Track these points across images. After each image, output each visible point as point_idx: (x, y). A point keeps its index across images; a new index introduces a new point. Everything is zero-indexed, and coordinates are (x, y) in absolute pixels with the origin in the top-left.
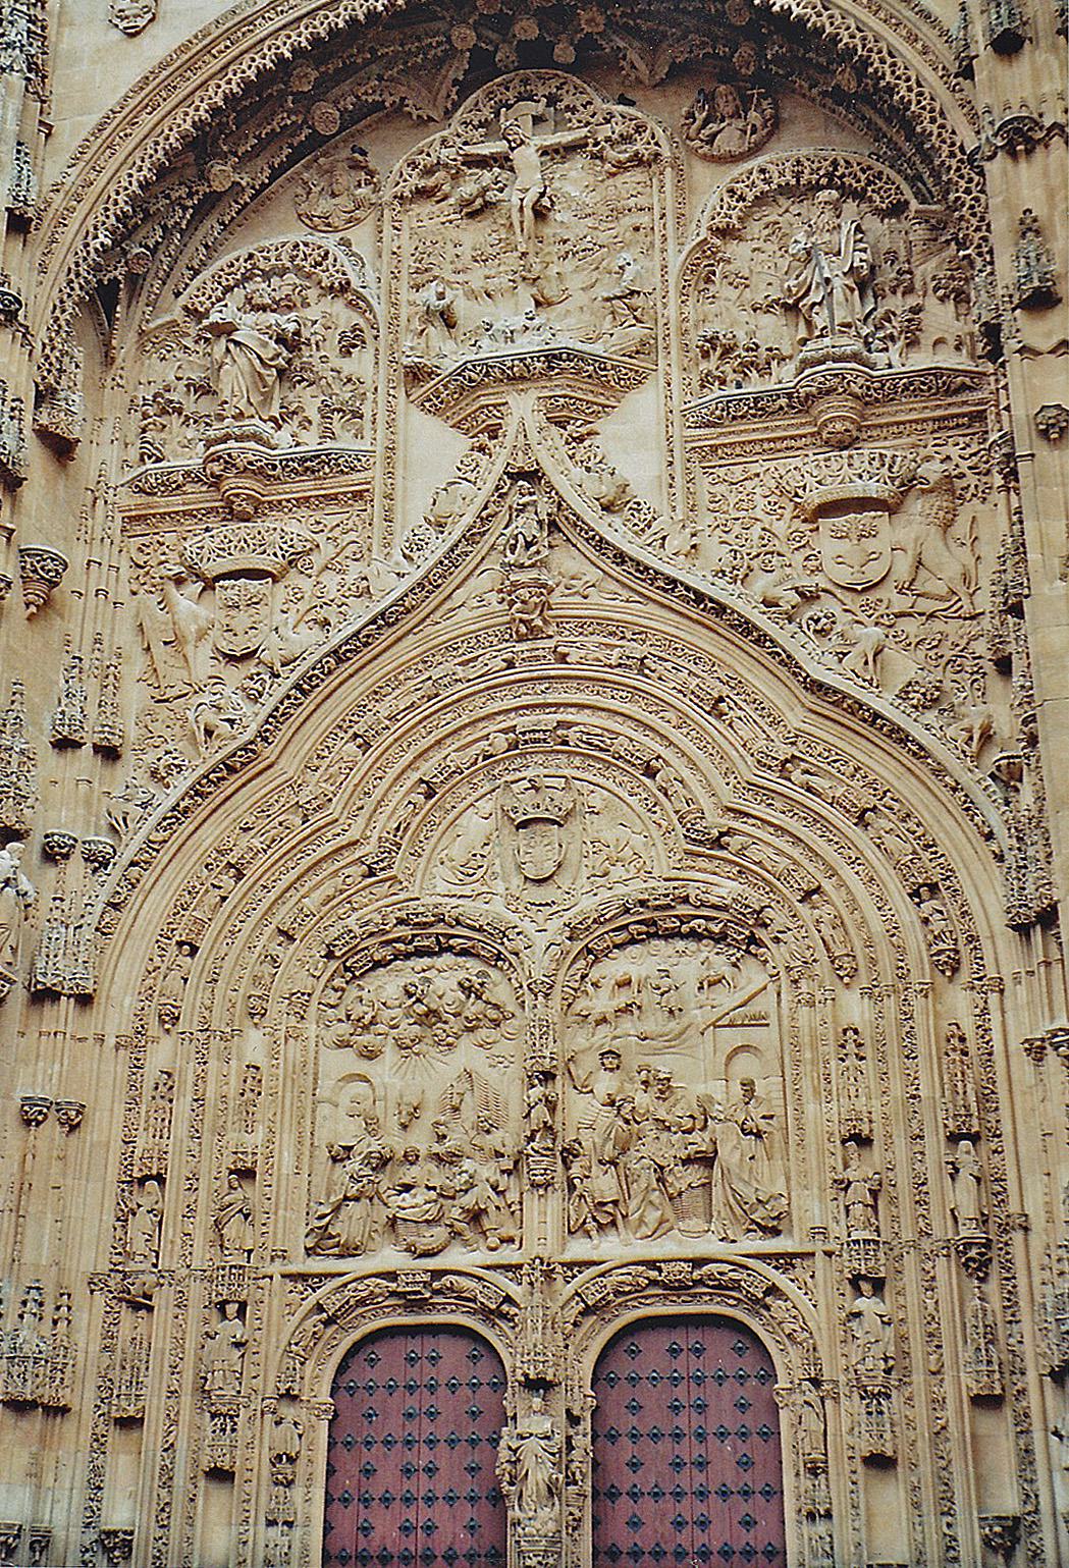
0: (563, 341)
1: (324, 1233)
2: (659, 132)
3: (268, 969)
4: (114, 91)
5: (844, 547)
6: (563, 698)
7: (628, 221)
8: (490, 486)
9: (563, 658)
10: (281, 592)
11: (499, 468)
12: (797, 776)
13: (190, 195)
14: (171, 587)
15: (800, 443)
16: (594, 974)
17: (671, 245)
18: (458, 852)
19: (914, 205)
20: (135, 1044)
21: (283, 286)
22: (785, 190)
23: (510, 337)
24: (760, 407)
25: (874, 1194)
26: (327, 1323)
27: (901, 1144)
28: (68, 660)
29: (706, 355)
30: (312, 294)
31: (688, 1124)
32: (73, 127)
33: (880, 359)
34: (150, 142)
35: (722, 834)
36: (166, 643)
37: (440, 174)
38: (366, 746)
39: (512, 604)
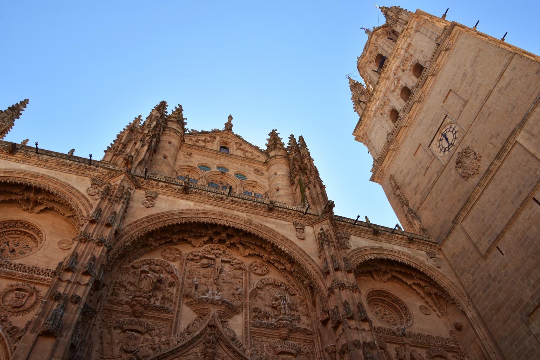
2: (246, 265)
4: (141, 216)
7: (238, 280)
8: (204, 326)
10: (142, 339)
11: (207, 323)
13: (143, 242)
14: (112, 329)
15: (274, 337)
17: (248, 288)
19: (298, 295)
21: (158, 268)
22: (271, 284)
23: (213, 295)
24: (268, 326)
29: (255, 312)
30: (164, 272)
32: (129, 220)
34: (145, 229)
36: (107, 343)
37: (198, 257)
39: (205, 357)
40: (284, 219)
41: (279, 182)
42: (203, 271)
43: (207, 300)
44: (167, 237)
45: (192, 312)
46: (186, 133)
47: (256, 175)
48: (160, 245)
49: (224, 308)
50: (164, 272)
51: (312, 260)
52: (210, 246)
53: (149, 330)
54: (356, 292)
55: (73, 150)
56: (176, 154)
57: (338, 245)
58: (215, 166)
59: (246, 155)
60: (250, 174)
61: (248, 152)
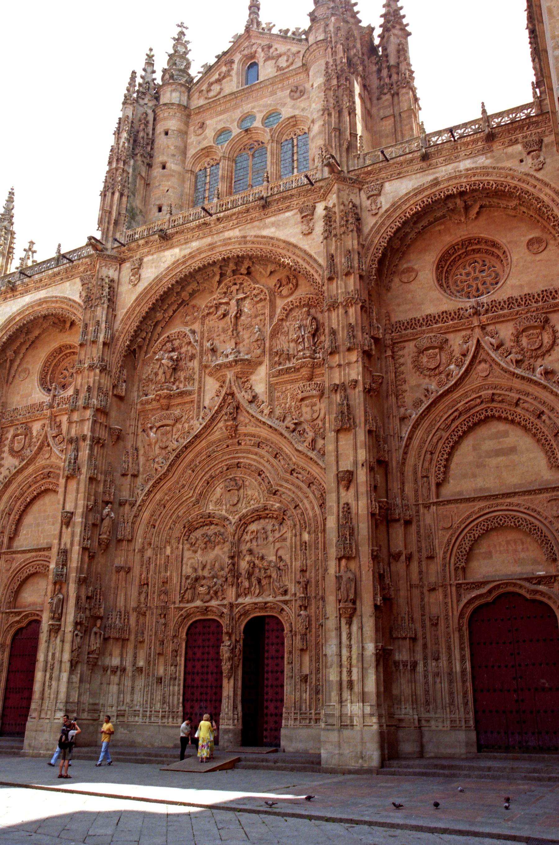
0: (242, 356)
1: (183, 597)
3: (171, 531)
5: (308, 409)
6: (240, 455)
7: (258, 318)
8: (221, 398)
9: (239, 444)
11: (223, 393)
12: (295, 474)
16: (247, 529)
18: (214, 499)
20: (142, 551)
22: (297, 306)
23: (227, 356)
25: (306, 585)
26: (184, 618)
27: (313, 571)
28: (125, 452)
31: (267, 567)
32: (121, 313)
33: (318, 355)
35: (276, 491)
38: (193, 471)
40: (288, 209)
41: (313, 105)
42: (222, 324)
43: (220, 365)
44: (175, 301)
45: (215, 381)
46: (195, 81)
47: (293, 102)
48: (174, 312)
49: (239, 367)
50: (183, 344)
51: (320, 265)
52: (226, 284)
53: (177, 420)
54: (352, 305)
55: (59, 246)
56: (179, 143)
57: (343, 229)
58: (236, 123)
59: (278, 66)
60: (284, 105)
61: (280, 56)
